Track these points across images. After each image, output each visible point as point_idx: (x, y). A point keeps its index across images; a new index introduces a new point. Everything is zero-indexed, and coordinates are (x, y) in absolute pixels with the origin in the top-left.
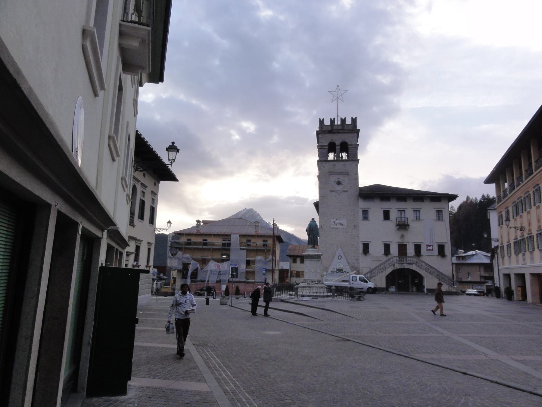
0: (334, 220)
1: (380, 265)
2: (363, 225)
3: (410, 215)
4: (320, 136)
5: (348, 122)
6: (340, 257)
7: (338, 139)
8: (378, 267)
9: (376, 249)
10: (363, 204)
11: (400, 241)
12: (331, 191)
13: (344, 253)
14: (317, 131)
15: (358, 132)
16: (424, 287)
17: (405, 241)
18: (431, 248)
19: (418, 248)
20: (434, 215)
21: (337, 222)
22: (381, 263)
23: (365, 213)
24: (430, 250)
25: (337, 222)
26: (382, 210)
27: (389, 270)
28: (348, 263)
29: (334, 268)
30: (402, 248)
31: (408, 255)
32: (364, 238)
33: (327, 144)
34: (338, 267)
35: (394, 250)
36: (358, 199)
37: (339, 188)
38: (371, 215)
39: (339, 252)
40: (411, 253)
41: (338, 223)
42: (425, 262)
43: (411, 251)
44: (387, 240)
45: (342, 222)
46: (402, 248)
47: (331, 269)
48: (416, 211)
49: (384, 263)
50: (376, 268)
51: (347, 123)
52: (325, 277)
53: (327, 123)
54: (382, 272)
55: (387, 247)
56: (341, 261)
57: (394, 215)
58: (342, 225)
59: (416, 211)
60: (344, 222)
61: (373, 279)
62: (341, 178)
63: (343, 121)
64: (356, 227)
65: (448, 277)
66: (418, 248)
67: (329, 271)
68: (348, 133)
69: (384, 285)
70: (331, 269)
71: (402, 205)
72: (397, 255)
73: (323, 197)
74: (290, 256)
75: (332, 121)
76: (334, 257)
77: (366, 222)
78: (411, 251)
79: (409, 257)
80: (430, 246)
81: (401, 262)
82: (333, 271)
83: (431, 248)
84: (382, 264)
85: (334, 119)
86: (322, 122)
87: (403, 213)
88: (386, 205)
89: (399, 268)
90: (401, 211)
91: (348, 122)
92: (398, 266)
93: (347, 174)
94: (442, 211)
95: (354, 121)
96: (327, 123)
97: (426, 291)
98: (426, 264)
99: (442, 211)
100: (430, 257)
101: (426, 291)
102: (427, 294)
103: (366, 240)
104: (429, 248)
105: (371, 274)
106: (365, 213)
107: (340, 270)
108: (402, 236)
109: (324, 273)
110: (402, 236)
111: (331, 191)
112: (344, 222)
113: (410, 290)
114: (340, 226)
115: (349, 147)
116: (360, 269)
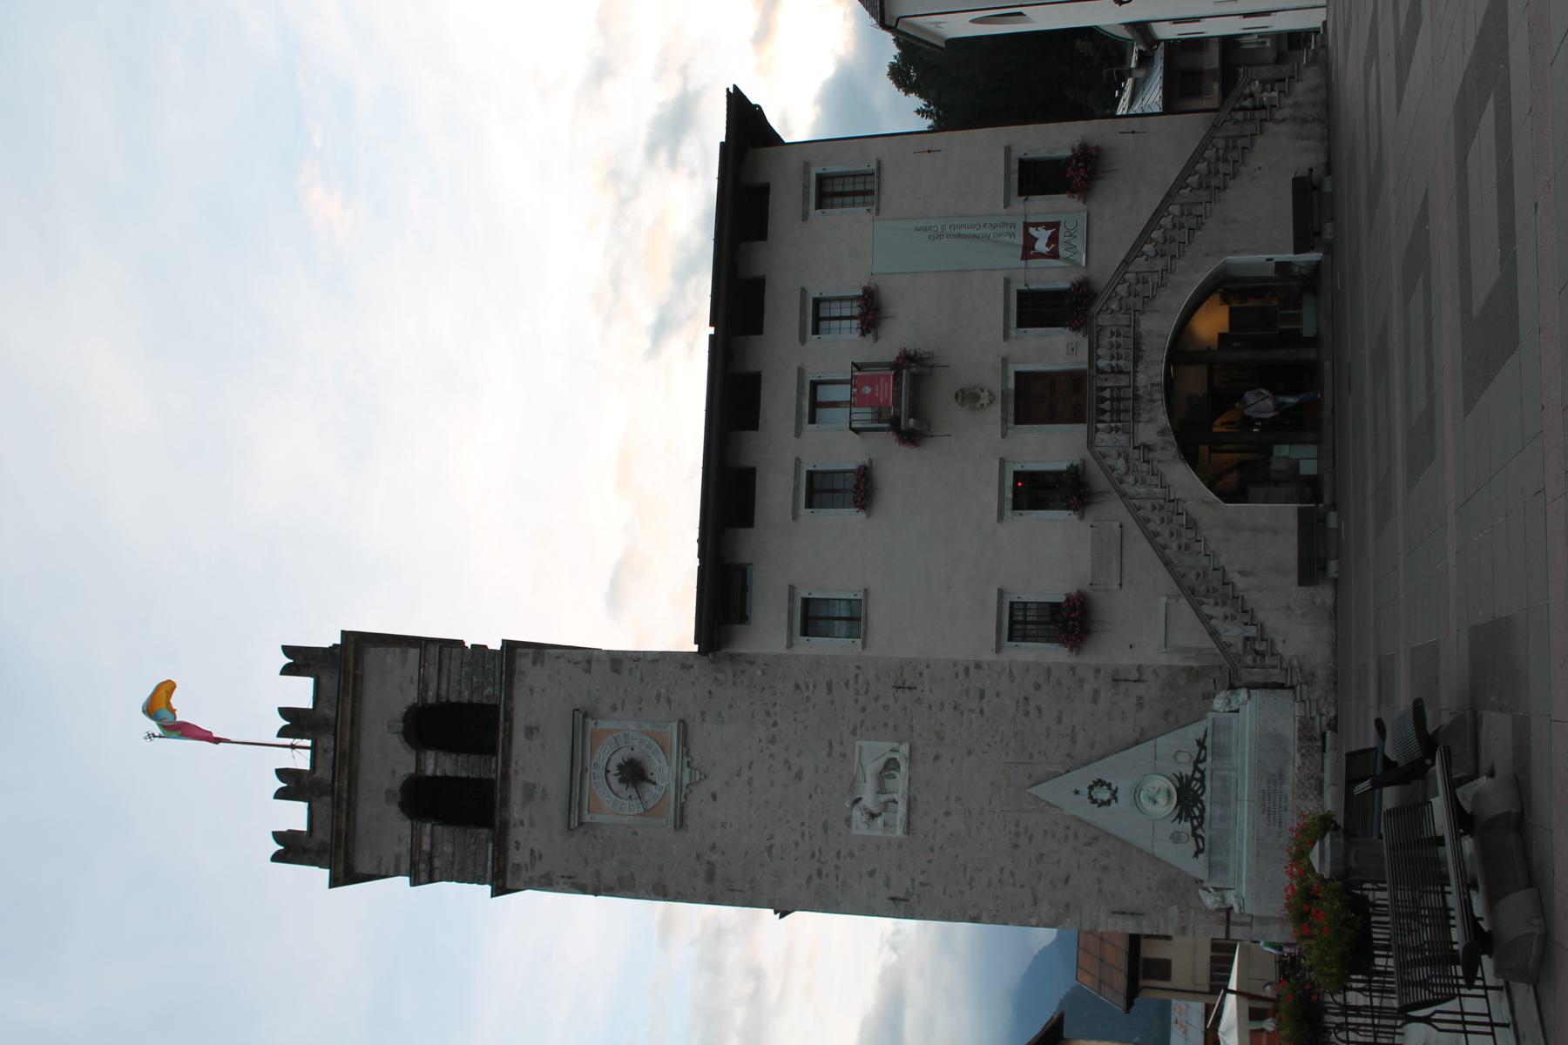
0: (857, 814)
1: (1152, 537)
2: (896, 635)
3: (840, 350)
4: (362, 867)
5: (301, 691)
6: (1101, 792)
7: (388, 760)
8: (1160, 550)
9: (1052, 555)
10: (767, 631)
11: (995, 412)
12: (680, 822)
13: (1074, 763)
14: (334, 883)
15: (355, 642)
16: (1282, 267)
17: (995, 383)
18: (1042, 236)
19: (1035, 309)
20: (845, 220)
21: (869, 799)
22: (1134, 530)
23: (812, 618)
24: (1053, 239)
25: (869, 799)
26: (803, 511)
27: (1183, 479)
28: (1137, 743)
29: (1176, 838)
30: (1036, 399)
31: (1080, 362)
32: (970, 635)
33: (404, 826)
34: (1165, 807)
35: (1052, 447)
36: (733, 658)
37: (663, 770)
38: (833, 586)
39: (1065, 794)
40: (1073, 350)
41: (881, 790)
42: (1126, 262)
43: (1055, 350)
44: (989, 494)
45: (872, 768)
46: (1036, 399)
47: (1181, 857)
48: (818, 316)
49: (1134, 510)
50: (1167, 563)
51: (306, 702)
52: (1231, 899)
53: (296, 816)
54: (1192, 524)
55: (1033, 491)
56: (1124, 786)
57: (837, 445)
58: (891, 765)
59: (817, 319)
60: (872, 753)
61: (1240, 583)
62: (605, 757)
63: (295, 723)
64: (904, 679)
65: (1215, 126)
66: (1035, 309)
67: (1197, 868)
68: (357, 698)
69: (1288, 513)
70: (1181, 857)
71: (779, 401)
72: (1081, 429)
73: (710, 876)
74: (1132, 992)
75: (292, 785)
76: (1098, 835)
77: (878, 617)
78: (1055, 350)
79: (1093, 357)
80: (1029, 241)
81: (1123, 409)
82: (1191, 846)
83: (1042, 236)
84: (1143, 523)
85: (282, 773)
86: (291, 849)
87: (825, 394)
88: (777, 493)
89: (1163, 419)
90: (815, 405)
91: (301, 691)
92: (1154, 425)
93: (581, 718)
94: (821, 179)
95: (300, 660)
96: (296, 816)
97: (1314, 256)
98: (1136, 250)
99: (821, 179)
100: (1093, 238)
101: (1314, 256)
102: (1330, 249)
103: (989, 624)
104: (1041, 246)
105: (1203, 588)
106: (812, 618)
107: (1188, 799)
108: (969, 397)
109: (1210, 901)
110: (969, 397)
111: (680, 822)
112: (872, 753)
113: (1310, 354)
114: (899, 784)
115: (431, 698)
116: (1177, 661)
